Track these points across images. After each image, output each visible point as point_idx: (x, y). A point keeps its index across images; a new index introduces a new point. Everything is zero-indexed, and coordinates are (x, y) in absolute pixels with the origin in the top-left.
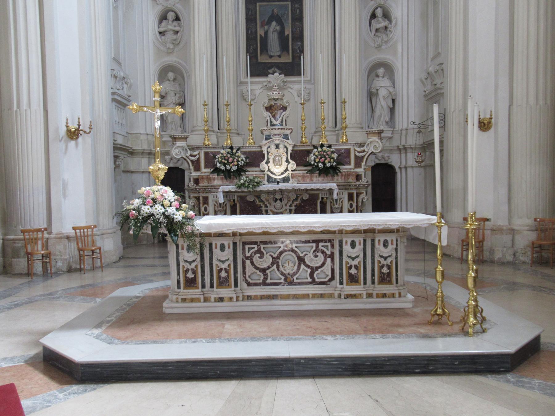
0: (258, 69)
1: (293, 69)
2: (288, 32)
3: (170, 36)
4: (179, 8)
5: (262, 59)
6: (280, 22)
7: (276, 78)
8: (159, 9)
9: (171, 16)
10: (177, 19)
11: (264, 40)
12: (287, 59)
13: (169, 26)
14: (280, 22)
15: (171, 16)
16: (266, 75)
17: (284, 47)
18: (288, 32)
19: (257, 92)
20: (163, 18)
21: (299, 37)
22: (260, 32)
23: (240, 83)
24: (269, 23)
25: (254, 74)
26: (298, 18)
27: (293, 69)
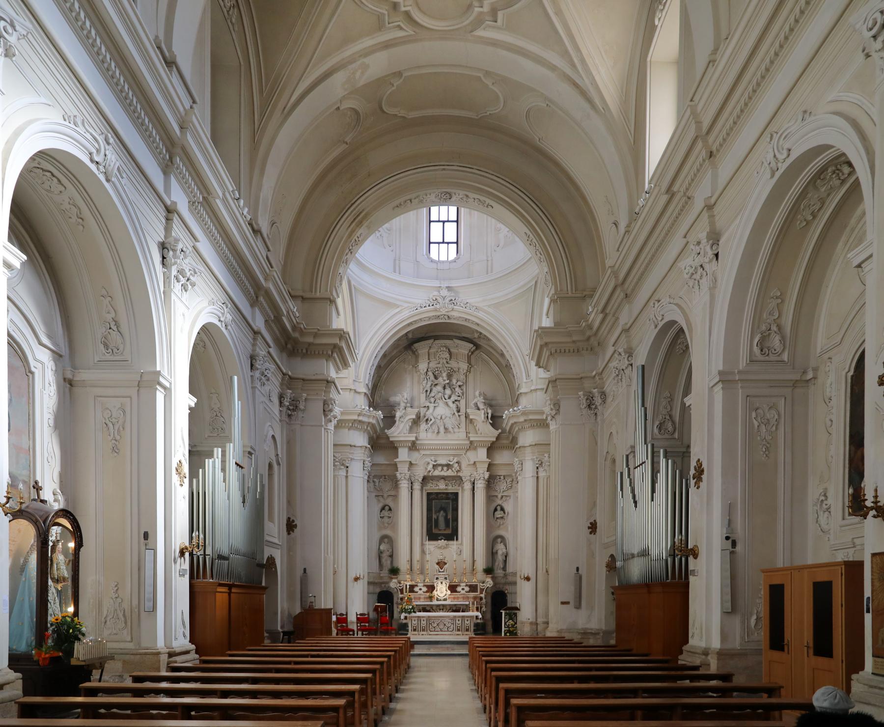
0: (432, 536)
1: (452, 535)
2: (450, 516)
3: (386, 520)
4: (392, 505)
5: (435, 531)
6: (446, 511)
7: (442, 542)
8: (381, 505)
9: (387, 508)
10: (390, 509)
11: (437, 521)
12: (449, 531)
13: (386, 513)
14: (446, 511)
15: (387, 508)
16: (437, 539)
17: (447, 525)
18: (450, 516)
19: (432, 549)
20: (383, 509)
21: (456, 519)
22: (434, 516)
23: (422, 545)
24: (439, 511)
25: (430, 539)
26: (455, 509)
27: (452, 535)
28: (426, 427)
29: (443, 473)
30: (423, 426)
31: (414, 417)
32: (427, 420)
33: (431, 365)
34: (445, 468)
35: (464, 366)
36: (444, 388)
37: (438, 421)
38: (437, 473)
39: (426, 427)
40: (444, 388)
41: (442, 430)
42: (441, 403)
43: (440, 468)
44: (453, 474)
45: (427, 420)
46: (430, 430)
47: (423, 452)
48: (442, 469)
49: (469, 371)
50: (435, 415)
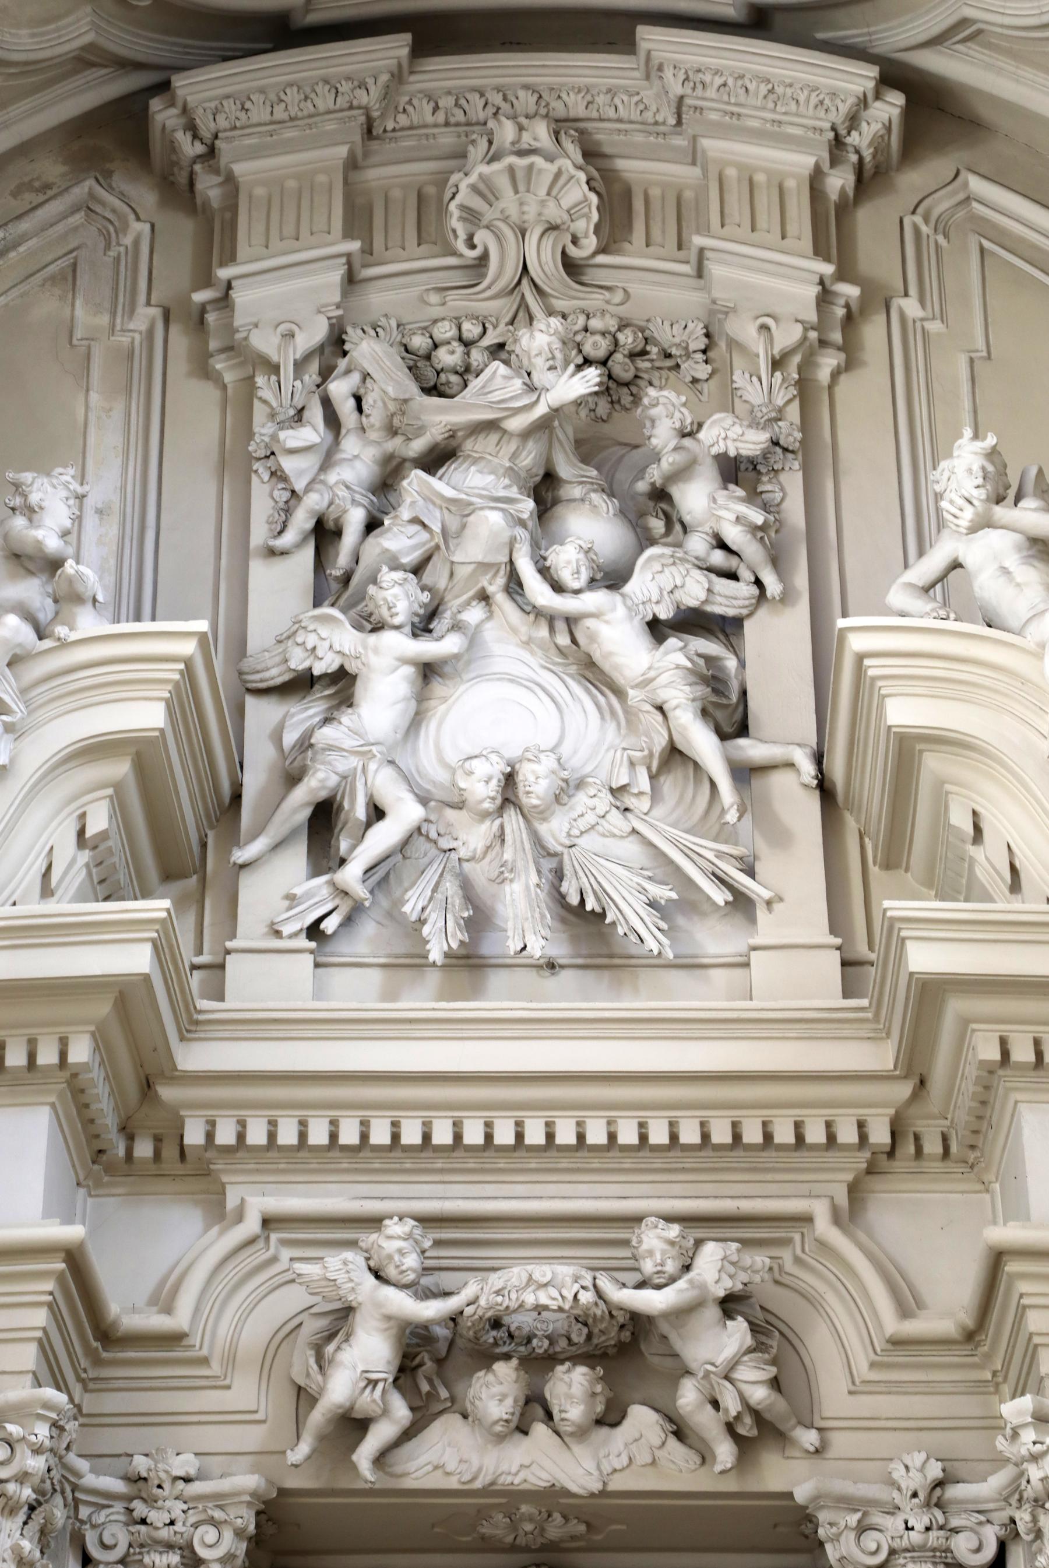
28: (316, 895)
29: (541, 1462)
30: (277, 885)
31: (148, 716)
32: (324, 820)
33: (380, 299)
34: (572, 1388)
35: (773, 284)
36: (545, 491)
37: (472, 837)
38: (451, 1457)
39: (316, 895)
40: (545, 491)
41: (523, 921)
42: (506, 644)
43: (496, 1390)
44: (676, 1472)
45: (324, 820)
46: (367, 940)
47: (257, 1198)
48: (534, 1409)
49: (841, 327)
50: (428, 759)
